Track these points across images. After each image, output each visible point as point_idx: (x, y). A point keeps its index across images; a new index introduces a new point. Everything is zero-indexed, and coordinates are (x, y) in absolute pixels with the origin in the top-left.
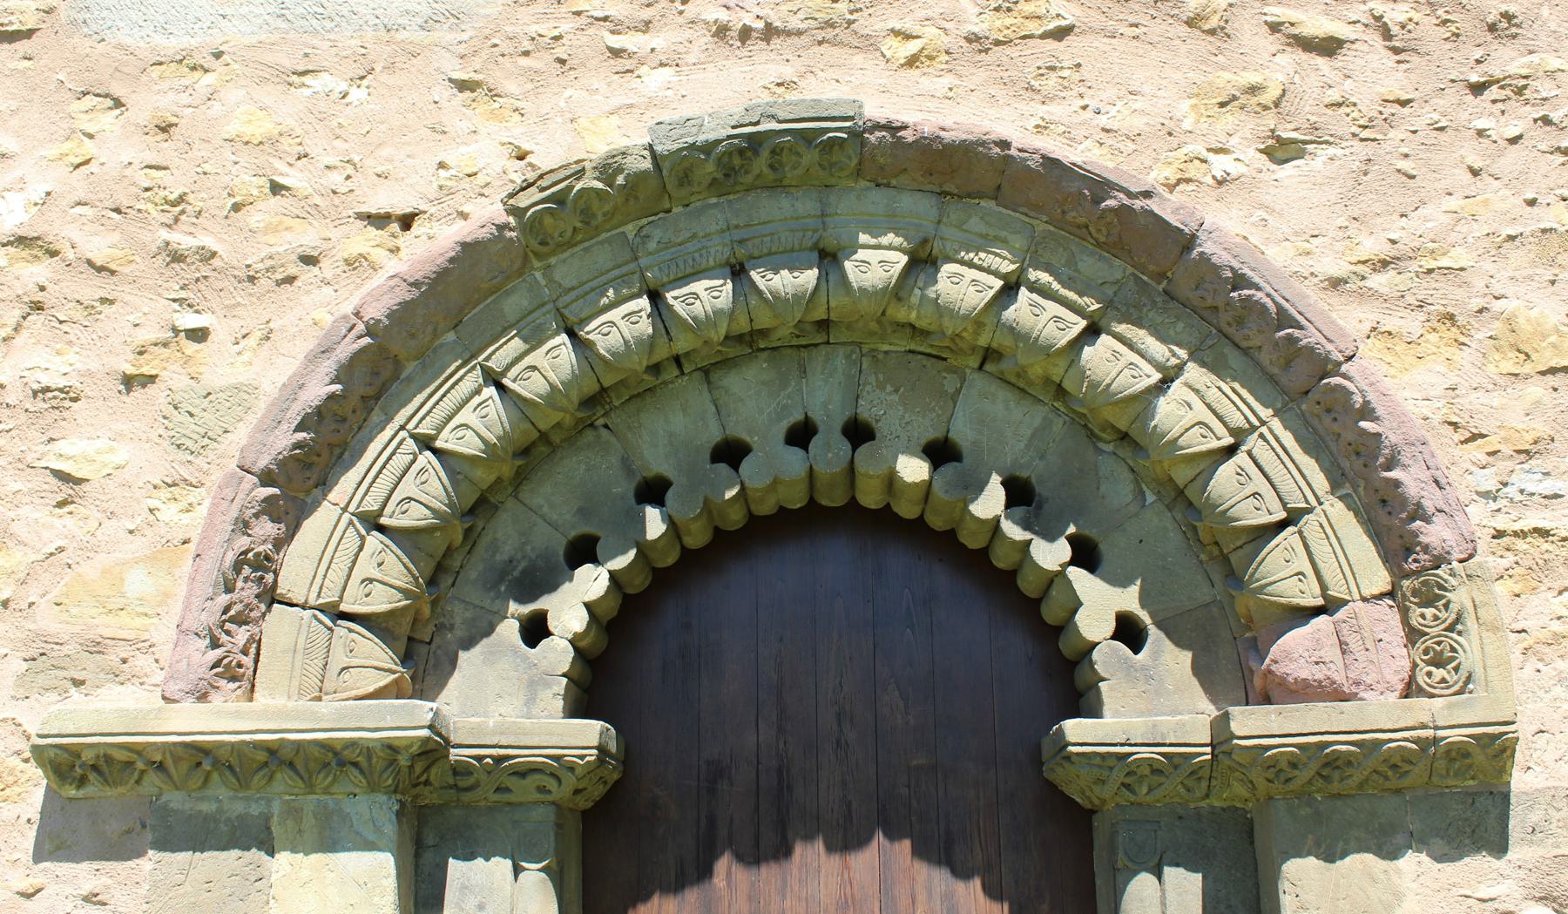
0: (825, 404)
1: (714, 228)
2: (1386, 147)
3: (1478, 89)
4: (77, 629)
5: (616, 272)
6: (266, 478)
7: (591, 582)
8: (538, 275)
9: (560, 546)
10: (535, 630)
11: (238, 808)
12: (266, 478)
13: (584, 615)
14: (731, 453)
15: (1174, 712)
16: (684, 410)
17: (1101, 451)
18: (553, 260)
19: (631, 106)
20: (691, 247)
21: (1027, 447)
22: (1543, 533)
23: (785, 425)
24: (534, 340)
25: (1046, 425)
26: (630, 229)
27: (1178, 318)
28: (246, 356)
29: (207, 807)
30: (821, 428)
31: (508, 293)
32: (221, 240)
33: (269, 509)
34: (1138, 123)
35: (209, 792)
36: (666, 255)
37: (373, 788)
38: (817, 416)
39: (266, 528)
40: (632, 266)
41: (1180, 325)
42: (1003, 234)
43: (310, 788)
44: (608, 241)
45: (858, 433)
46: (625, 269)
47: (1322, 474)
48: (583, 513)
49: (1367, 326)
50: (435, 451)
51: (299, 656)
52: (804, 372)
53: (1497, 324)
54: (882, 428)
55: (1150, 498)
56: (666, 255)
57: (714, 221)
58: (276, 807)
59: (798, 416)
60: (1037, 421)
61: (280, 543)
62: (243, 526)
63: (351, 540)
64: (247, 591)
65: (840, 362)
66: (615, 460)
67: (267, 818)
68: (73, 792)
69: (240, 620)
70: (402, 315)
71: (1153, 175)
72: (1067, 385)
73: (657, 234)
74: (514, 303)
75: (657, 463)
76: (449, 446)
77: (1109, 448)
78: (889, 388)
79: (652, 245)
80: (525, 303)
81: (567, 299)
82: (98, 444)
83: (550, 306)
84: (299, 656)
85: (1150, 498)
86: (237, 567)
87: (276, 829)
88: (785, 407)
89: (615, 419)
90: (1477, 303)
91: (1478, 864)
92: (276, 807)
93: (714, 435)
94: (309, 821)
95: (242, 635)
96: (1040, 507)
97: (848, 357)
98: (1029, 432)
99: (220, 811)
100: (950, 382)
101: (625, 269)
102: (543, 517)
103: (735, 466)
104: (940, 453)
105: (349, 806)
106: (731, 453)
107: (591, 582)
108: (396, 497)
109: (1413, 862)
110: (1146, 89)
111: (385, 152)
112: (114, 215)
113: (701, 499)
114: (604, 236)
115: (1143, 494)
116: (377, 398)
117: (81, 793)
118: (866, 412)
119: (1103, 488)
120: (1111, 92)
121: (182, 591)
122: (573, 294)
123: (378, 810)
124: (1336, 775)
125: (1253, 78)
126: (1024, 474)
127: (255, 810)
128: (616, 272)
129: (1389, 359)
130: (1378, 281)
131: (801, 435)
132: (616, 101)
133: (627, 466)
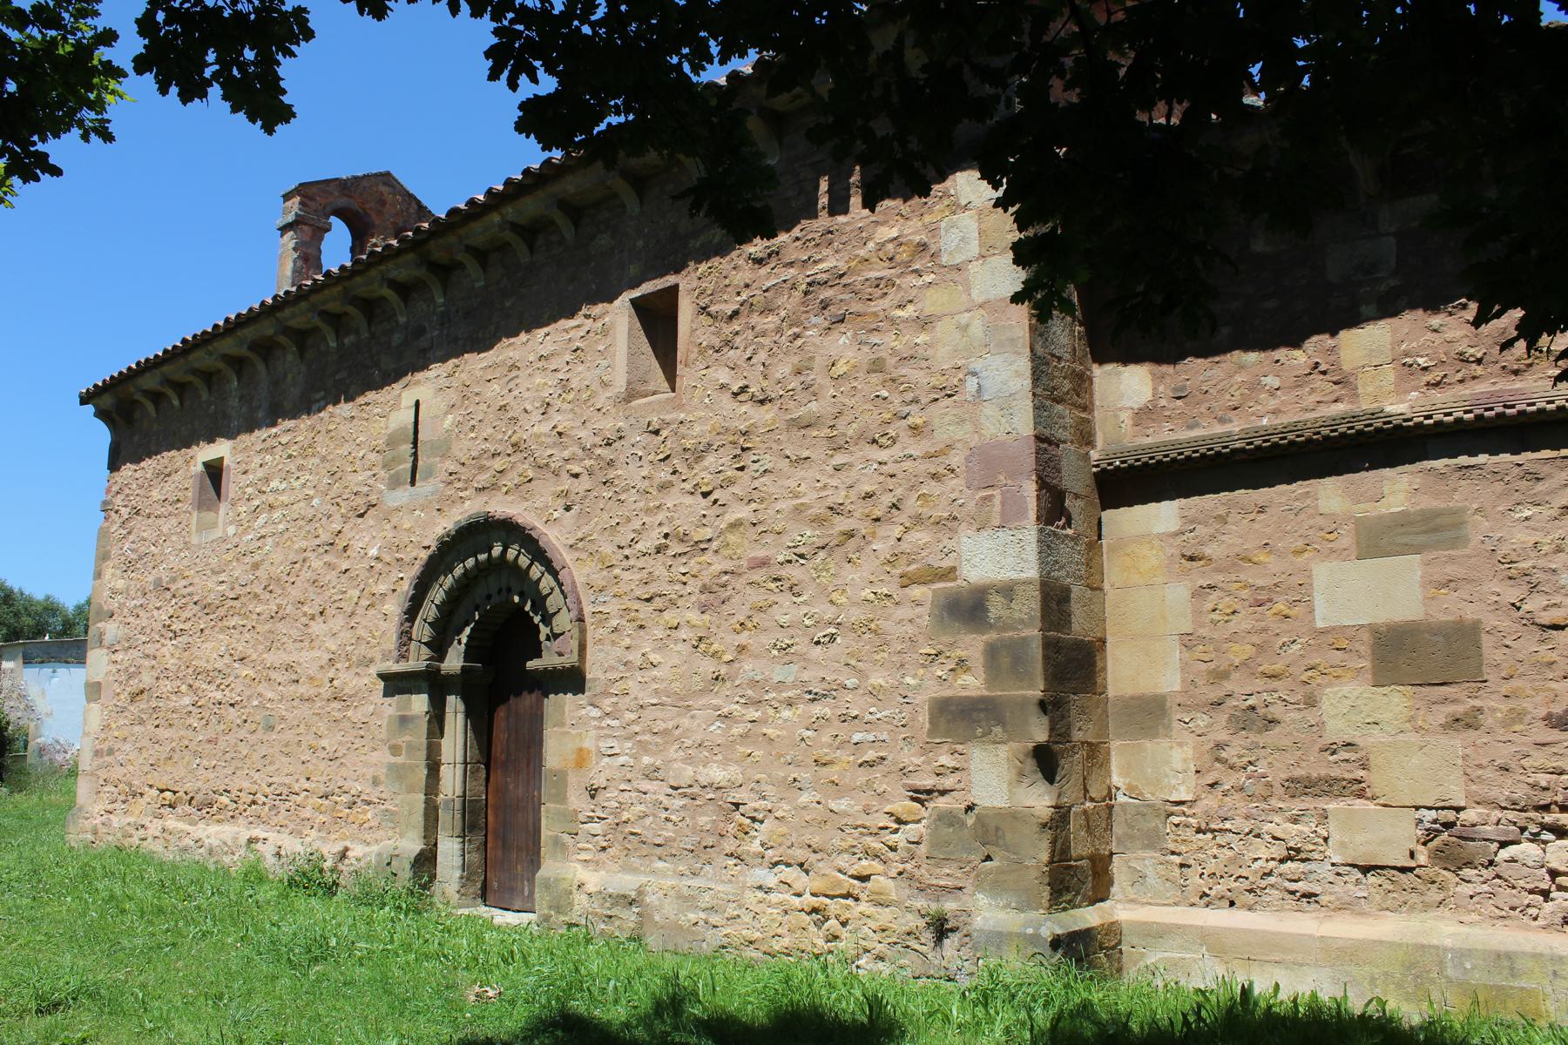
3: (605, 483)
6: (405, 614)
7: (468, 630)
10: (460, 643)
12: (405, 614)
14: (489, 597)
22: (601, 612)
24: (446, 576)
33: (407, 620)
39: (408, 624)
47: (1163, 503)
61: (411, 627)
62: (402, 624)
64: (405, 639)
69: (404, 645)
70: (422, 573)
74: (442, 567)
86: (402, 633)
91: (580, 695)
95: (405, 648)
104: (521, 595)
106: (489, 597)
107: (468, 630)
109: (569, 695)
123: (424, 685)
125: (562, 488)
130: (580, 545)
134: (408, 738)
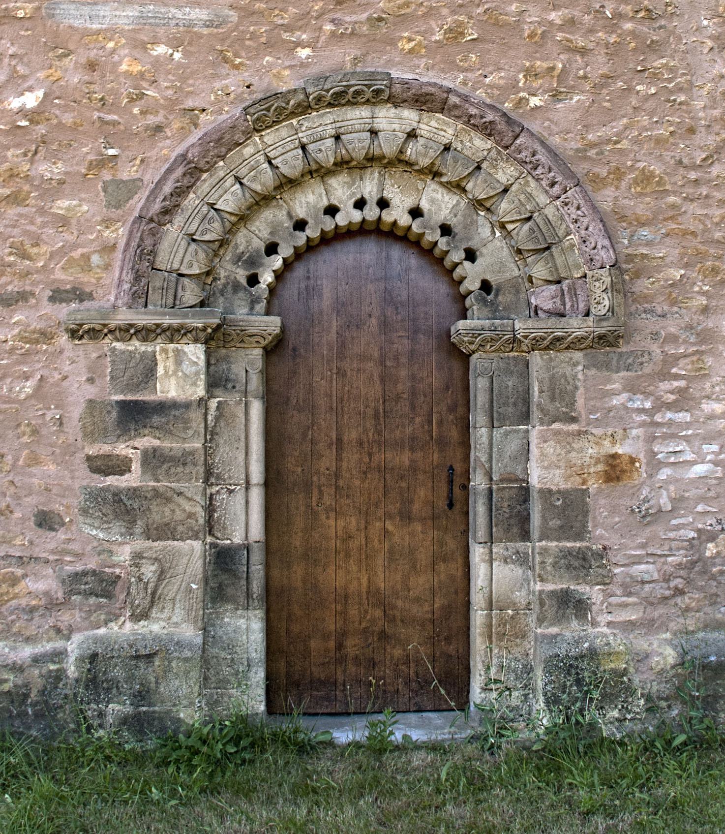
0: (370, 192)
1: (329, 122)
2: (601, 96)
4: (72, 278)
5: (289, 139)
8: (257, 139)
9: (262, 246)
11: (143, 349)
13: (273, 274)
14: (332, 211)
15: (501, 319)
16: (313, 193)
17: (478, 214)
18: (263, 133)
19: (294, 66)
20: (319, 129)
21: (450, 213)
23: (353, 200)
25: (458, 203)
26: (294, 121)
27: (512, 165)
28: (135, 168)
29: (130, 348)
30: (369, 202)
31: (245, 146)
32: (121, 117)
34: (502, 82)
35: (131, 342)
36: (309, 132)
37: (196, 341)
38: (367, 196)
40: (295, 137)
41: (512, 169)
42: (445, 128)
43: (171, 341)
44: (286, 126)
45: (383, 204)
46: (292, 138)
48: (271, 233)
49: (586, 171)
50: (215, 210)
51: (165, 291)
52: (361, 179)
53: (637, 173)
54: (393, 203)
55: (498, 234)
56: (309, 132)
57: (328, 119)
58: (158, 348)
59: (359, 196)
60: (455, 202)
63: (184, 243)
65: (376, 175)
66: (285, 213)
67: (154, 352)
68: (77, 342)
71: (506, 105)
72: (466, 188)
73: (306, 124)
75: (301, 212)
76: (222, 208)
77: (483, 213)
78: (396, 186)
79: (304, 129)
80: (252, 151)
81: (269, 149)
82: (74, 203)
83: (262, 152)
84: (165, 291)
85: (498, 234)
87: (158, 357)
88: (354, 193)
89: (286, 196)
90: (629, 163)
92: (158, 348)
93: (325, 203)
94: (171, 354)
96: (454, 237)
97: (379, 173)
98: (451, 206)
99: (136, 349)
100: (420, 185)
101: (292, 138)
102: (256, 235)
103: (333, 216)
105: (186, 348)
108: (200, 229)
110: (506, 67)
111: (191, 82)
112: (73, 104)
113: (320, 230)
114: (284, 124)
115: (495, 233)
116: (191, 187)
117: (80, 342)
118: (386, 194)
119: (479, 230)
120: (490, 69)
121: (117, 264)
122: (272, 147)
124: (558, 344)
126: (449, 223)
127: (150, 349)
128: (289, 139)
129: (593, 184)
131: (360, 204)
132: (287, 63)
133: (290, 215)
134: (147, 441)
